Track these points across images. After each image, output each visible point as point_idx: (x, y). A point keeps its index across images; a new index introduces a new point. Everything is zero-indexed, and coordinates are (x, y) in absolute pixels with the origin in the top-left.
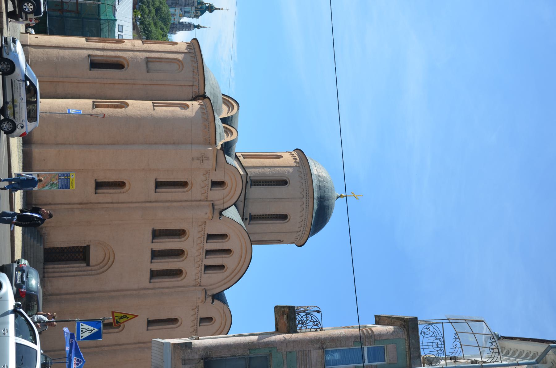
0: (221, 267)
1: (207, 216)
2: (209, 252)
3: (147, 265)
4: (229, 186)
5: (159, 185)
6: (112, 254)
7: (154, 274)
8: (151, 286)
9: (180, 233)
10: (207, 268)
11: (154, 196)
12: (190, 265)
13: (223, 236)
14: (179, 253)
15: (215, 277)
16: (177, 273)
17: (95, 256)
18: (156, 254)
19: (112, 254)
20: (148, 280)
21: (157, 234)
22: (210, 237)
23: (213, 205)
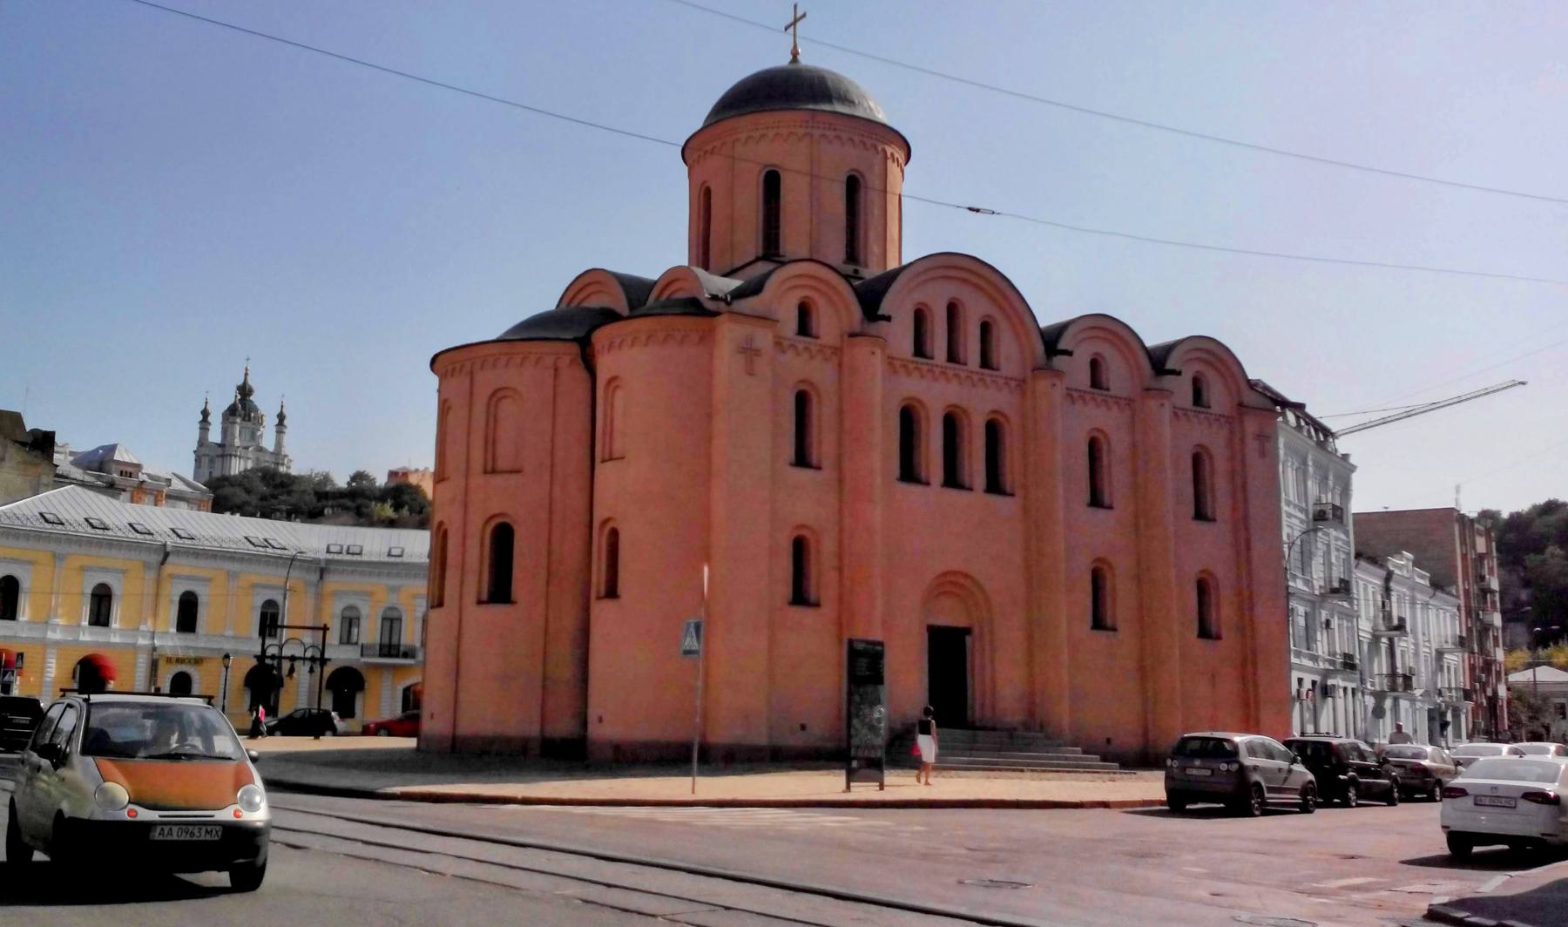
0: (986, 328)
1: (878, 352)
2: (952, 357)
3: (975, 500)
4: (807, 293)
5: (802, 459)
6: (949, 578)
7: (995, 485)
8: (1019, 493)
9: (909, 419)
10: (986, 362)
11: (828, 474)
12: (980, 400)
13: (920, 317)
14: (952, 424)
15: (1007, 349)
16: (993, 431)
17: (951, 616)
18: (952, 479)
19: (949, 578)
20: (1008, 499)
21: (909, 472)
22: (920, 349)
23: (852, 335)
